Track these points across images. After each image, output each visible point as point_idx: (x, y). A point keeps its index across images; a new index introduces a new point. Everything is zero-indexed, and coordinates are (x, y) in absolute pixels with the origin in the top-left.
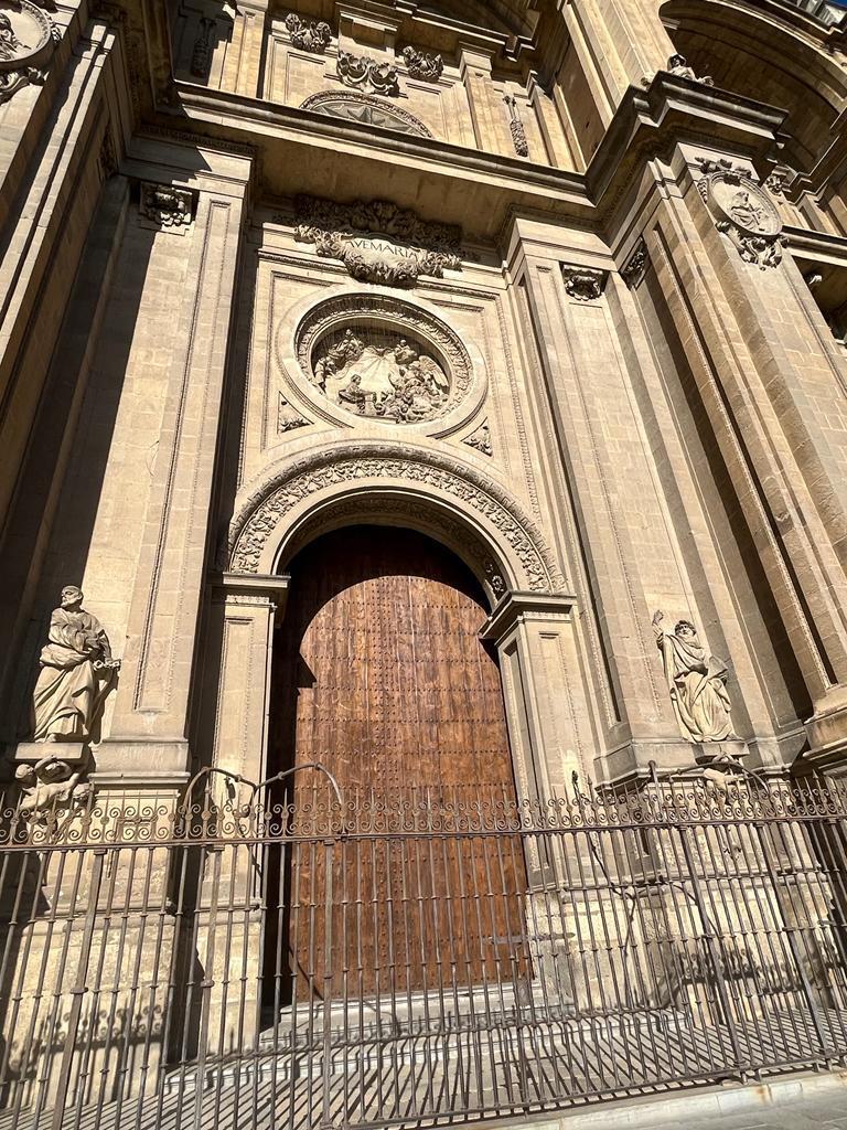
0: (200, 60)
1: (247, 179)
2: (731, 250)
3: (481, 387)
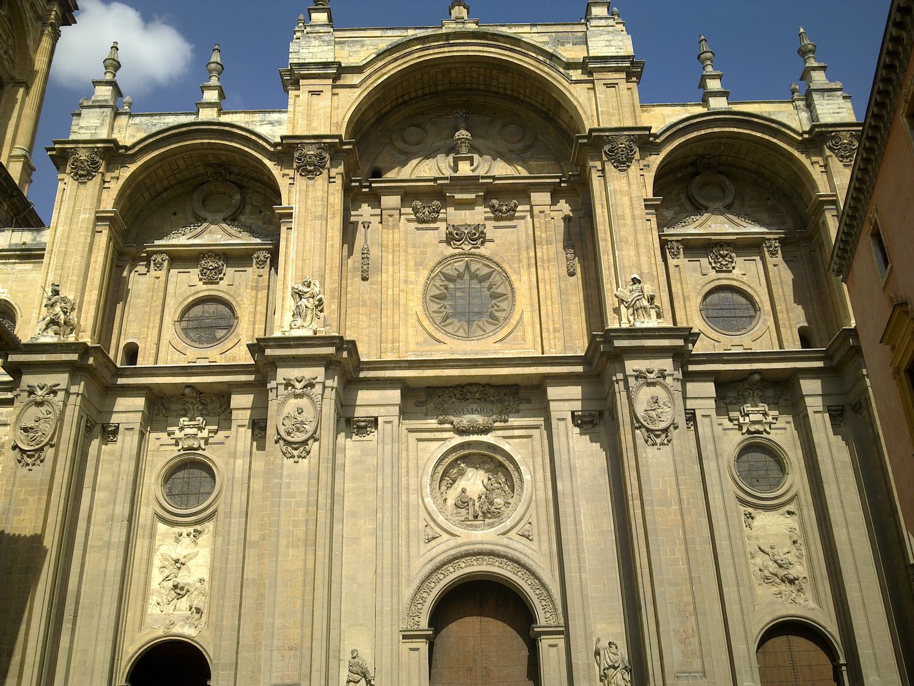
0: (365, 267)
1: (399, 402)
2: (640, 441)
3: (528, 495)
